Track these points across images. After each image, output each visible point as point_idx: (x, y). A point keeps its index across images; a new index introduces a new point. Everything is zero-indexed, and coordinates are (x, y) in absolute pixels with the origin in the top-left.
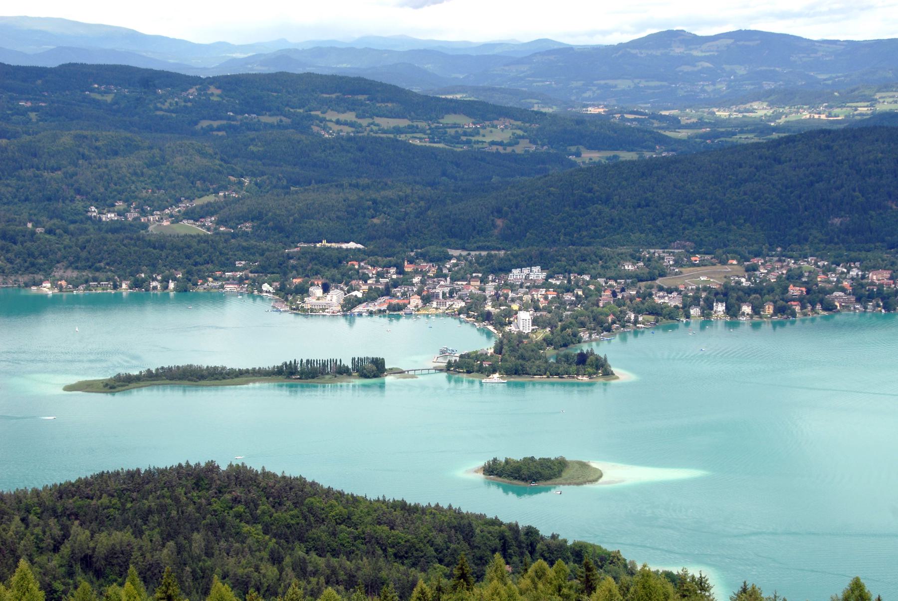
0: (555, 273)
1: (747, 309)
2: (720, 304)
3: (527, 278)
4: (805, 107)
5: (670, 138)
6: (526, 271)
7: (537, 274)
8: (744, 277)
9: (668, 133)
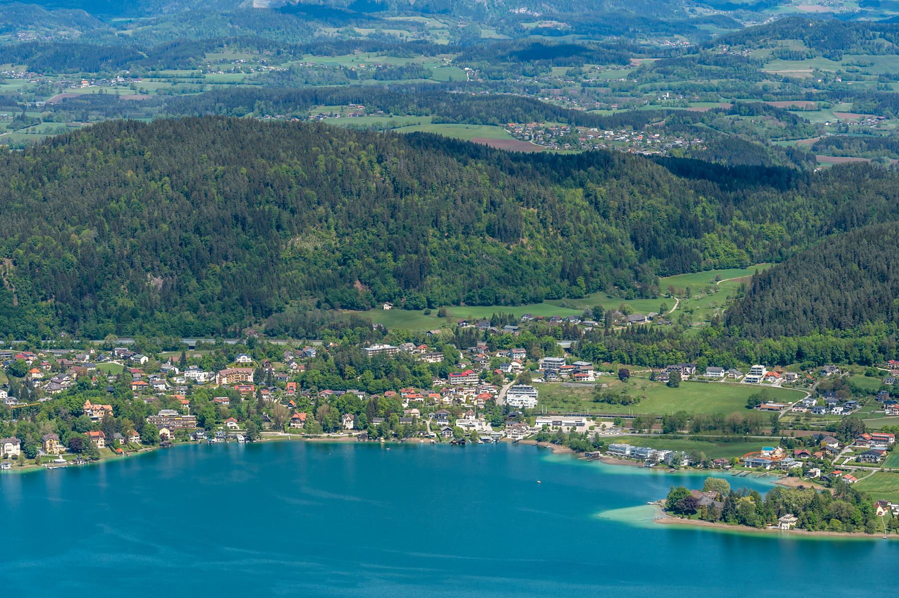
4: (91, 74)
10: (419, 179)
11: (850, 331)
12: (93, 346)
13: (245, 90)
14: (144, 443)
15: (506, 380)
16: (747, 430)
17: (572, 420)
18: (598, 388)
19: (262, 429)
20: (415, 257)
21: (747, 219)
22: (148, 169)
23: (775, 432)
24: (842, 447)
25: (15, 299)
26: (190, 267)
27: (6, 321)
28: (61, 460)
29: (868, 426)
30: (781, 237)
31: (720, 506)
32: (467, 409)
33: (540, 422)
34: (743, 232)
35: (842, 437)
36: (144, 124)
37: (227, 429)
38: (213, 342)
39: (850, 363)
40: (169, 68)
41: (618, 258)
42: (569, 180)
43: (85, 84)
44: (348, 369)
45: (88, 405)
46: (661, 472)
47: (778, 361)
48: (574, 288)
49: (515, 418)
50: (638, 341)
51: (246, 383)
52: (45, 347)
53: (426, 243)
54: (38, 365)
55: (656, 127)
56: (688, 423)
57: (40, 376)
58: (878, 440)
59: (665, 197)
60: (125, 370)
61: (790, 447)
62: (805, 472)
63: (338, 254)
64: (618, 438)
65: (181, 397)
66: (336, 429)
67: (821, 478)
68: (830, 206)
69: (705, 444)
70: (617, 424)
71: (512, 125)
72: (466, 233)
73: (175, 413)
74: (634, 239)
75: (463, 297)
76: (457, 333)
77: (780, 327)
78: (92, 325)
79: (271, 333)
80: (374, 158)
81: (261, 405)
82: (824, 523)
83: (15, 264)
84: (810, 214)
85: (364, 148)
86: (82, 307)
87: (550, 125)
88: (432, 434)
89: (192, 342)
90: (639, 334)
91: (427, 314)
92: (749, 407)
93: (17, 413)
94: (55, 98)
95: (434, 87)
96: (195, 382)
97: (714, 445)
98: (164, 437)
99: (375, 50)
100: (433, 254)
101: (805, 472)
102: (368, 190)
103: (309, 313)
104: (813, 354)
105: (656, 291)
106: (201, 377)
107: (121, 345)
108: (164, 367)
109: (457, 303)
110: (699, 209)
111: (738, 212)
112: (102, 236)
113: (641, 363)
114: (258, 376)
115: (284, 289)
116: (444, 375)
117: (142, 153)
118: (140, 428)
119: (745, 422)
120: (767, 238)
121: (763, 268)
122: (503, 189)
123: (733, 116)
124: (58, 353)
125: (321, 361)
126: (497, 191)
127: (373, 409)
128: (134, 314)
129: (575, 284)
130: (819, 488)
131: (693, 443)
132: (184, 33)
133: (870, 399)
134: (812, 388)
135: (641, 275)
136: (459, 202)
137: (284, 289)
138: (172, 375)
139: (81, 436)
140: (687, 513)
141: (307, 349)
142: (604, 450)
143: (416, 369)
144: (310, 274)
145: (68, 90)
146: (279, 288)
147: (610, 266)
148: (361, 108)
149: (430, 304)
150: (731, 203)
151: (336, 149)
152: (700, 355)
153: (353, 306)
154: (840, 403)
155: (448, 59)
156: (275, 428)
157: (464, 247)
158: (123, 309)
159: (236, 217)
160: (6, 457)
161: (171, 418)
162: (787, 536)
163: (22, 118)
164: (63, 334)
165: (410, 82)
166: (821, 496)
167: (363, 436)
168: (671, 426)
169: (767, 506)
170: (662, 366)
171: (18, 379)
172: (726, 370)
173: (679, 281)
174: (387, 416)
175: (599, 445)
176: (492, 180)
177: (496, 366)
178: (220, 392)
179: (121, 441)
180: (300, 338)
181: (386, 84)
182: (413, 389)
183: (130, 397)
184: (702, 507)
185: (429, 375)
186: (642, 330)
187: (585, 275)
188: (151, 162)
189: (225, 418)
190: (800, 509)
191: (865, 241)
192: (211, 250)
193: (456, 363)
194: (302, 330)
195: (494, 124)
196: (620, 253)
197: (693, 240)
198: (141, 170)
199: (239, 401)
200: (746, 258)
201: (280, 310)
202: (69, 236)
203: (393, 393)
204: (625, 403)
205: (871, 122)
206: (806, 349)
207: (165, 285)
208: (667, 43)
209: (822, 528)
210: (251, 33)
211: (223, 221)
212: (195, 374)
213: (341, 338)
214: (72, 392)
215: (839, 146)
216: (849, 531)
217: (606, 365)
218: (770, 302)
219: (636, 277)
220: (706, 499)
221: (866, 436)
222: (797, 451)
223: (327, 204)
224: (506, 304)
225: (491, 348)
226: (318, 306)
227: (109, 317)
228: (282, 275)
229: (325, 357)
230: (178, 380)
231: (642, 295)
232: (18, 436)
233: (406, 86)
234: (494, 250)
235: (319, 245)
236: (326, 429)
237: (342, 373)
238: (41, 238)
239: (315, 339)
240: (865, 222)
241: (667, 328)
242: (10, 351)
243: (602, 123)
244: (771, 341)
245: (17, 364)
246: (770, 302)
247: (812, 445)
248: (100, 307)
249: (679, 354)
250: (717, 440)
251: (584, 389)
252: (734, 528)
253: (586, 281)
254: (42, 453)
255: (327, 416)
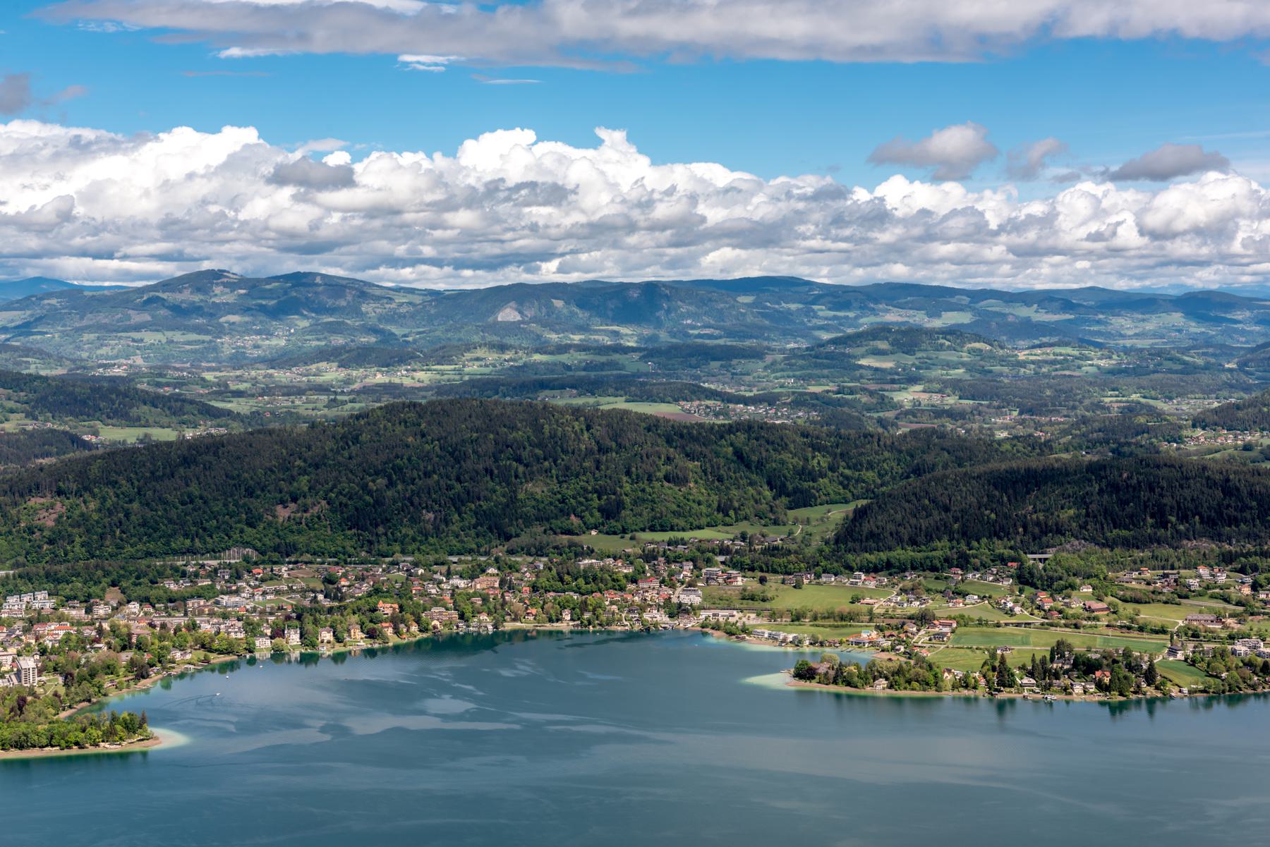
0: (68, 598)
1: (327, 636)
2: (292, 632)
3: (28, 608)
5: (217, 409)
6: (26, 598)
7: (43, 601)
8: (322, 592)
9: (213, 403)
10: (616, 442)
11: (923, 547)
12: (384, 562)
13: (492, 380)
14: (420, 631)
15: (678, 584)
16: (851, 619)
17: (726, 613)
18: (745, 590)
19: (505, 621)
20: (613, 497)
21: (849, 468)
22: (423, 436)
23: (871, 620)
24: (919, 630)
25: (329, 529)
26: (454, 505)
27: (323, 545)
28: (362, 643)
29: (937, 615)
30: (874, 481)
31: (832, 673)
32: (651, 606)
33: (703, 615)
34: (847, 478)
35: (919, 623)
36: (420, 404)
37: (480, 621)
38: (470, 558)
39: (924, 570)
40: (438, 364)
41: (758, 497)
42: (723, 442)
43: (379, 376)
44: (567, 578)
45: (381, 605)
46: (790, 649)
47: (872, 569)
48: (727, 519)
49: (687, 612)
50: (773, 555)
51: (493, 588)
52: (350, 563)
53: (621, 487)
54: (345, 576)
55: (785, 403)
56: (809, 614)
57: (347, 583)
58: (944, 625)
59: (791, 453)
60: (407, 579)
61: (881, 630)
62: (893, 649)
63: (559, 496)
64: (759, 625)
65: (447, 597)
66: (558, 620)
67: (904, 653)
68: (908, 458)
69: (821, 629)
70: (758, 615)
71: (682, 403)
72: (650, 479)
73: (443, 610)
74: (769, 483)
75: (647, 525)
76: (644, 551)
77: (874, 545)
78: (383, 547)
79: (511, 552)
80: (584, 427)
81: (504, 603)
82: (907, 685)
83: (328, 503)
84: (894, 464)
85: (577, 420)
86: (377, 534)
87: (709, 403)
88: (626, 623)
89: (455, 559)
90: (773, 551)
91: (622, 537)
92: (852, 603)
93: (330, 610)
94: (356, 386)
95: (627, 376)
96: (457, 587)
97: (828, 629)
98: (435, 627)
99: (584, 350)
100: (626, 495)
101: (893, 649)
102: (580, 450)
103: (538, 537)
104: (897, 564)
105: (785, 520)
106: (462, 583)
107: (404, 561)
108: (435, 576)
109: (643, 530)
110: (815, 461)
111: (843, 464)
112: (391, 484)
113: (775, 572)
114: (502, 583)
115: (520, 521)
116: (634, 581)
117: (419, 425)
118: (418, 621)
119: (849, 613)
120: (864, 481)
121: (862, 503)
122: (676, 448)
123: (839, 396)
124: (360, 568)
125: (547, 571)
126: (672, 450)
127: (584, 606)
128: (414, 540)
129: (727, 515)
130: (903, 659)
131: (812, 628)
132: (449, 339)
133: (939, 596)
134: (897, 589)
135: (775, 509)
136: (645, 458)
137: (520, 521)
138: (440, 582)
139: (376, 626)
140: (809, 679)
141: (537, 563)
142: (749, 634)
143: (615, 577)
144: (539, 510)
145: (367, 380)
146: (517, 520)
147: (752, 502)
148: (574, 391)
149: (624, 531)
150: (838, 457)
151: (557, 421)
152: (818, 565)
153: (569, 532)
154: (917, 599)
155: (636, 356)
156: (514, 620)
157: (648, 490)
158: (406, 536)
159: (486, 470)
160: (322, 642)
161: (440, 613)
162: (881, 694)
163: (334, 400)
164: (363, 554)
165: (609, 373)
166: (904, 666)
167: (577, 625)
168: (797, 617)
169: (866, 673)
170: (790, 574)
171: (331, 586)
172: (836, 575)
173: (802, 513)
174: (594, 610)
175: (745, 630)
176: (668, 442)
177: (671, 575)
178: (475, 594)
179: (405, 630)
180: (531, 555)
181: (593, 374)
182: (612, 592)
183: (411, 598)
184: (820, 674)
185: (624, 581)
186: (776, 548)
187: (735, 509)
188: (426, 430)
189: (479, 613)
190: (890, 675)
191: (933, 483)
192: (468, 493)
193: (644, 572)
194: (533, 550)
195: (669, 402)
196: (759, 493)
197: (811, 484)
198: (419, 437)
199: (488, 601)
200: (849, 495)
201: (517, 535)
202: (367, 484)
203: (598, 595)
204: (764, 600)
205: (936, 399)
206: (893, 561)
207: (435, 518)
208: (792, 345)
209: (905, 688)
210: (495, 339)
211: (477, 473)
212: (457, 581)
213: (561, 555)
214: (370, 595)
215: (915, 416)
216: (924, 690)
217: (749, 573)
218: (867, 527)
219: (771, 511)
220: (823, 669)
221: (936, 622)
222: (887, 633)
223: (551, 460)
224: (679, 530)
225: (668, 561)
226: (545, 532)
227: (396, 541)
228: (519, 511)
229: (550, 569)
230: (444, 586)
231: (776, 523)
232: (331, 626)
233: (607, 376)
234: (669, 492)
235: (545, 489)
236: (551, 620)
237: (561, 580)
238: (346, 485)
239: (542, 556)
240: (933, 469)
241: (794, 547)
242: (326, 566)
243: (746, 401)
244: (867, 555)
245: (330, 575)
246: (867, 527)
247: (897, 629)
248: (389, 534)
249: (802, 565)
250: (830, 626)
251: (734, 590)
252: (843, 689)
253: (736, 513)
254: (348, 639)
255: (552, 611)
